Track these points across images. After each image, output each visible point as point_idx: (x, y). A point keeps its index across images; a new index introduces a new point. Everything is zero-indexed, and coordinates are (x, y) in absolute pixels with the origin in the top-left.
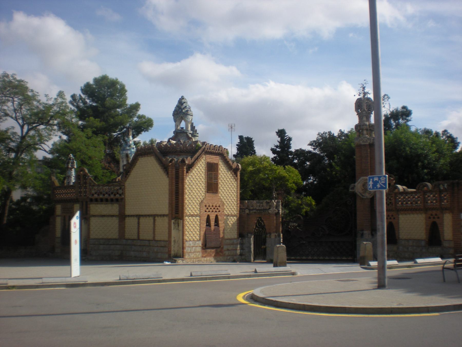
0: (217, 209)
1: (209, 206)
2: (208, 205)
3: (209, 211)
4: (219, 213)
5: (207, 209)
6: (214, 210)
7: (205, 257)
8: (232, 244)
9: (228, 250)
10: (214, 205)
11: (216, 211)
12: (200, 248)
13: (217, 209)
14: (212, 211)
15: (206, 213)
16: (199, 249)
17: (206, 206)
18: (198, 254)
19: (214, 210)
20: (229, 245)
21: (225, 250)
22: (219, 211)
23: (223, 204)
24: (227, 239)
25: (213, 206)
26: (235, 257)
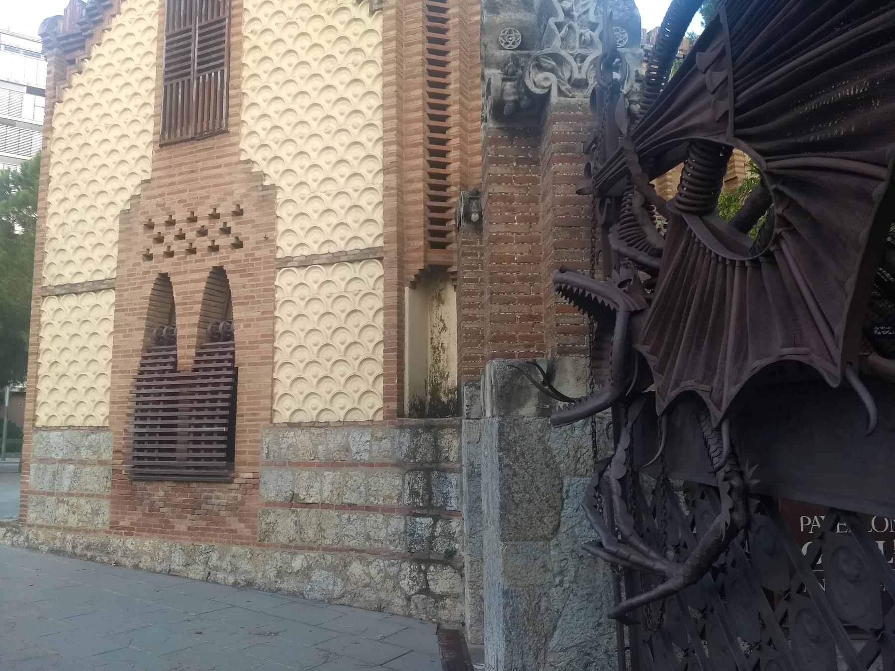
0: (226, 231)
1: (171, 223)
2: (160, 219)
3: (170, 254)
4: (238, 254)
5: (159, 240)
6: (202, 243)
7: (129, 531)
8: (333, 464)
9: (293, 502)
10: (204, 211)
11: (214, 249)
12: (104, 471)
13: (226, 231)
14: (192, 251)
15: (148, 264)
16: (96, 480)
17: (150, 226)
18: (86, 506)
19: (202, 243)
20: (307, 465)
21: (269, 504)
22: (238, 245)
23: (267, 196)
24: (291, 425)
25: (193, 219)
26: (356, 569)
